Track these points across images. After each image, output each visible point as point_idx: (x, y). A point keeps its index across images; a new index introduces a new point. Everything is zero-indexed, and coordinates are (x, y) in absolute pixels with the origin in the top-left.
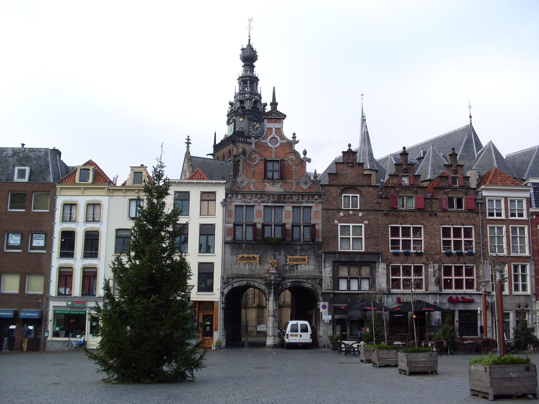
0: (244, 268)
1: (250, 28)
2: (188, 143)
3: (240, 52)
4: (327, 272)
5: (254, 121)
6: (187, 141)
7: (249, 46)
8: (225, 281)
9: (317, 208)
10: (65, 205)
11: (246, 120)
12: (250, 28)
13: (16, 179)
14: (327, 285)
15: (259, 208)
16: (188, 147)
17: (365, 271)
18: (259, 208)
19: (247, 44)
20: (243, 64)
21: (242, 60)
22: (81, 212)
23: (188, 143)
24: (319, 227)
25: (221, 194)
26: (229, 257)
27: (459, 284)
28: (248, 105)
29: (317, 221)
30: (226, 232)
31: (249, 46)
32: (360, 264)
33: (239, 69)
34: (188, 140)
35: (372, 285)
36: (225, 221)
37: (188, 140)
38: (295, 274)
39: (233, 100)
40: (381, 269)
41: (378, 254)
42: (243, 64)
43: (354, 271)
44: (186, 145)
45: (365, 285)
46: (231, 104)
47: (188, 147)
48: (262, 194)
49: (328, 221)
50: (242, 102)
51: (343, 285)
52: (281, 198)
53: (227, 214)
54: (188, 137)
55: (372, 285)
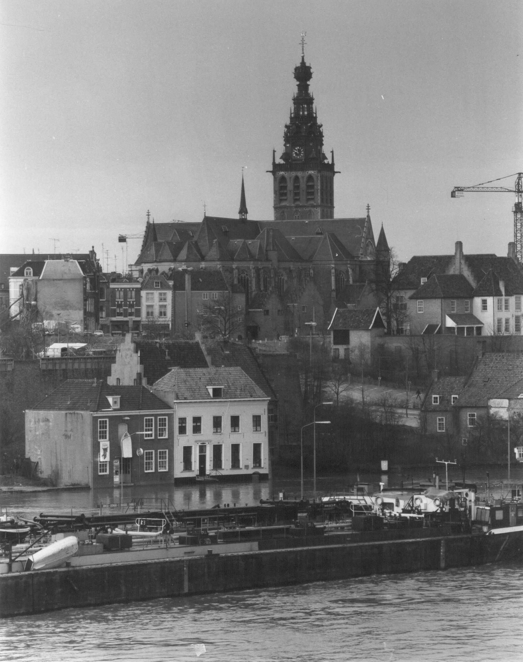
1: (303, 44)
2: (368, 209)
6: (367, 208)
7: (303, 63)
16: (368, 212)
19: (301, 61)
20: (298, 83)
21: (296, 79)
23: (368, 209)
31: (303, 63)
34: (368, 206)
37: (368, 206)
42: (298, 83)
44: (367, 211)
47: (368, 212)
54: (368, 204)
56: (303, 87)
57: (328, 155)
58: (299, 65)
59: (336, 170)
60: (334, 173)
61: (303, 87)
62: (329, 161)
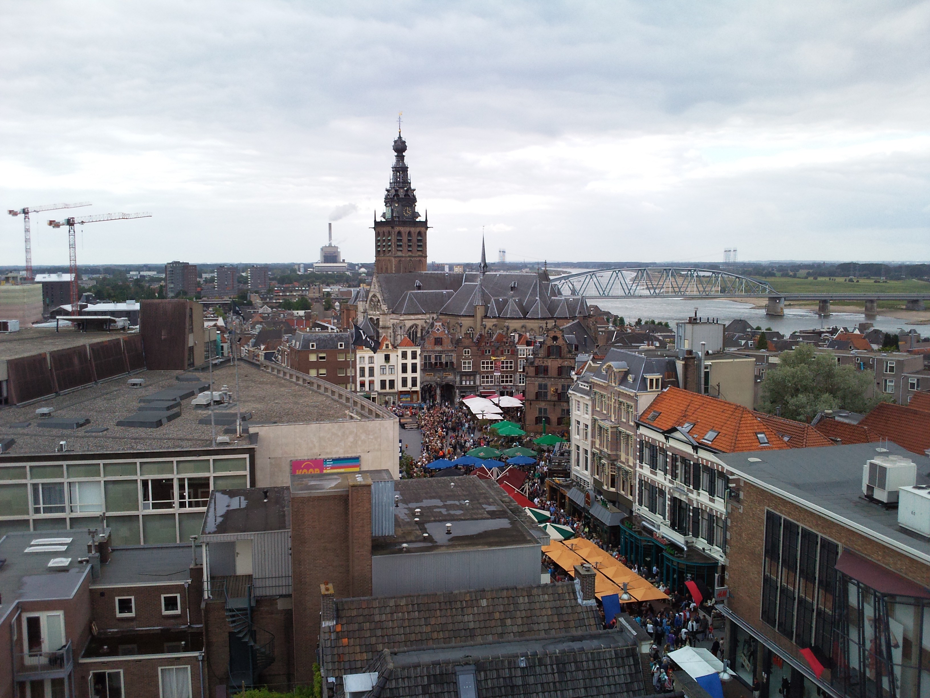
0: (428, 378)
1: (400, 121)
3: (393, 144)
4: (458, 379)
5: (406, 206)
7: (400, 137)
8: (421, 383)
9: (454, 355)
10: (360, 357)
11: (400, 206)
12: (400, 121)
13: (339, 348)
14: (458, 384)
15: (433, 356)
17: (472, 378)
18: (433, 356)
22: (367, 360)
24: (455, 362)
25: (419, 352)
26: (422, 375)
27: (507, 382)
28: (401, 193)
29: (454, 361)
30: (421, 365)
31: (400, 137)
32: (470, 375)
33: (392, 158)
35: (475, 383)
36: (421, 361)
38: (446, 380)
39: (388, 187)
40: (478, 377)
41: (476, 372)
42: (396, 154)
43: (468, 377)
45: (472, 383)
46: (387, 190)
48: (434, 351)
49: (458, 360)
50: (396, 191)
51: (464, 383)
52: (441, 352)
53: (421, 359)
55: (475, 383)
56: (400, 157)
57: (422, 213)
58: (396, 139)
59: (428, 226)
60: (427, 228)
61: (400, 157)
62: (422, 219)
